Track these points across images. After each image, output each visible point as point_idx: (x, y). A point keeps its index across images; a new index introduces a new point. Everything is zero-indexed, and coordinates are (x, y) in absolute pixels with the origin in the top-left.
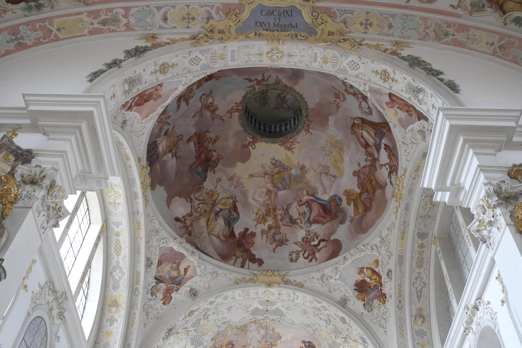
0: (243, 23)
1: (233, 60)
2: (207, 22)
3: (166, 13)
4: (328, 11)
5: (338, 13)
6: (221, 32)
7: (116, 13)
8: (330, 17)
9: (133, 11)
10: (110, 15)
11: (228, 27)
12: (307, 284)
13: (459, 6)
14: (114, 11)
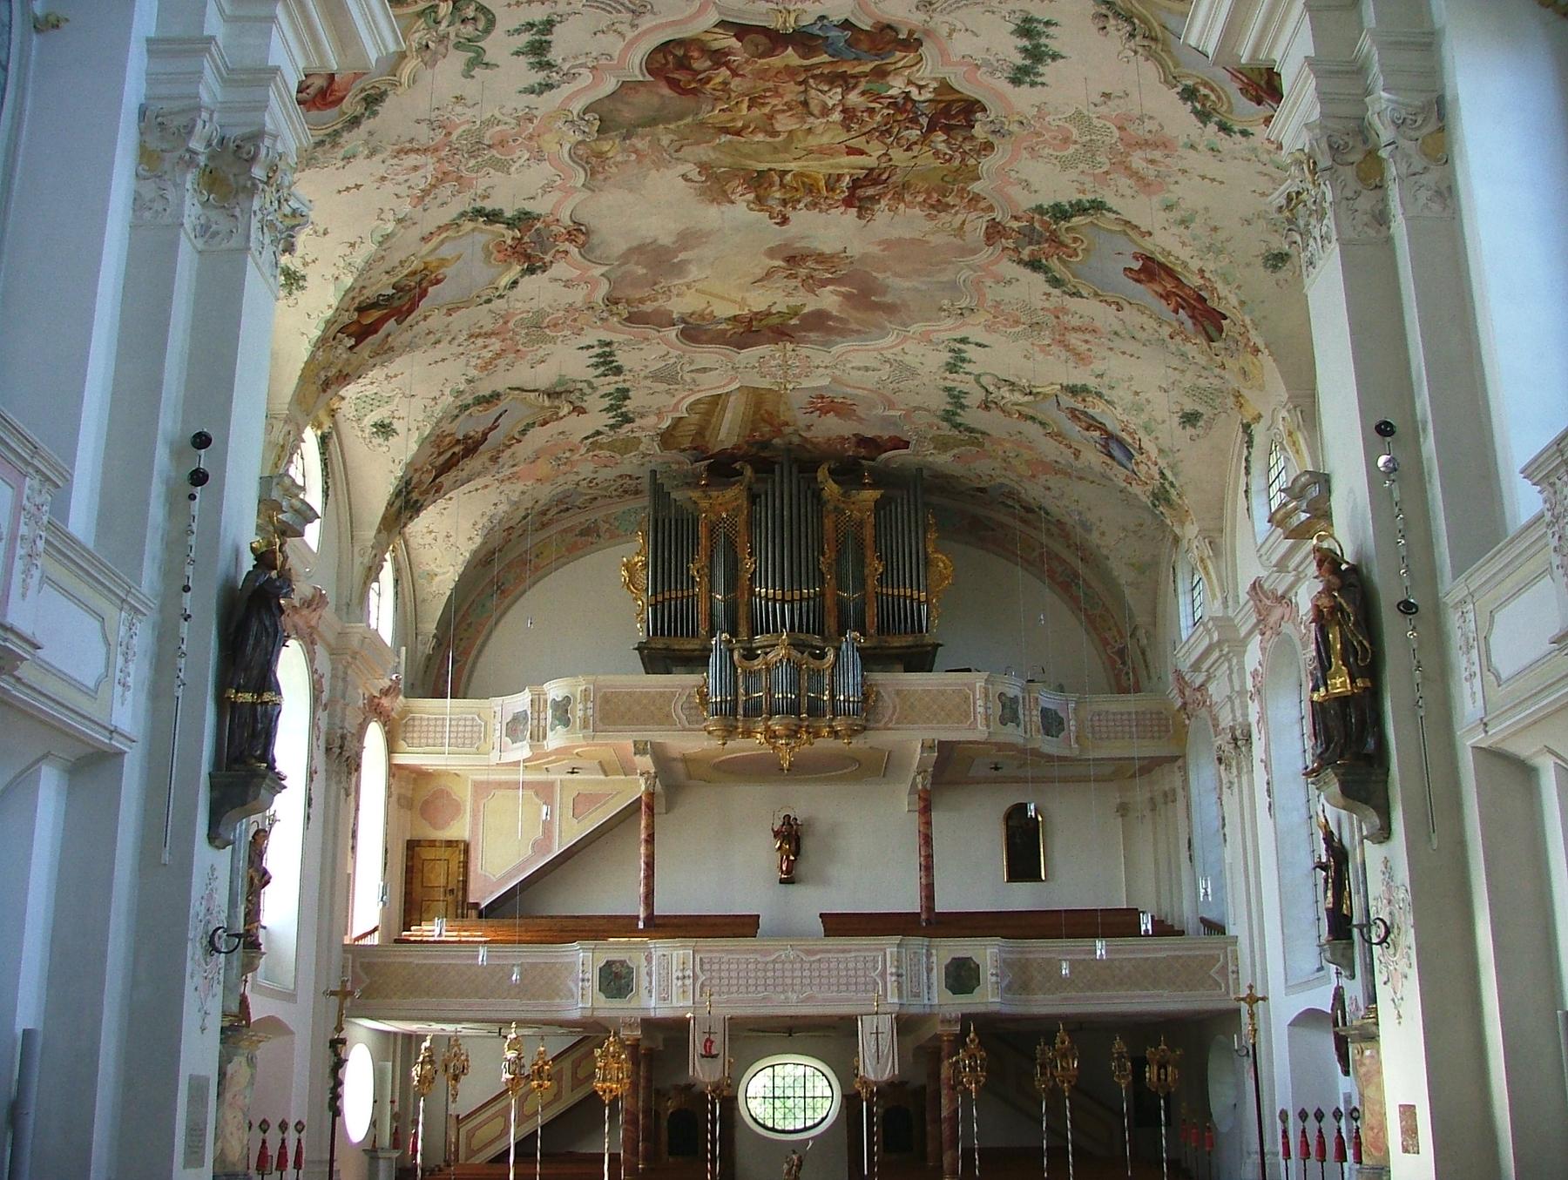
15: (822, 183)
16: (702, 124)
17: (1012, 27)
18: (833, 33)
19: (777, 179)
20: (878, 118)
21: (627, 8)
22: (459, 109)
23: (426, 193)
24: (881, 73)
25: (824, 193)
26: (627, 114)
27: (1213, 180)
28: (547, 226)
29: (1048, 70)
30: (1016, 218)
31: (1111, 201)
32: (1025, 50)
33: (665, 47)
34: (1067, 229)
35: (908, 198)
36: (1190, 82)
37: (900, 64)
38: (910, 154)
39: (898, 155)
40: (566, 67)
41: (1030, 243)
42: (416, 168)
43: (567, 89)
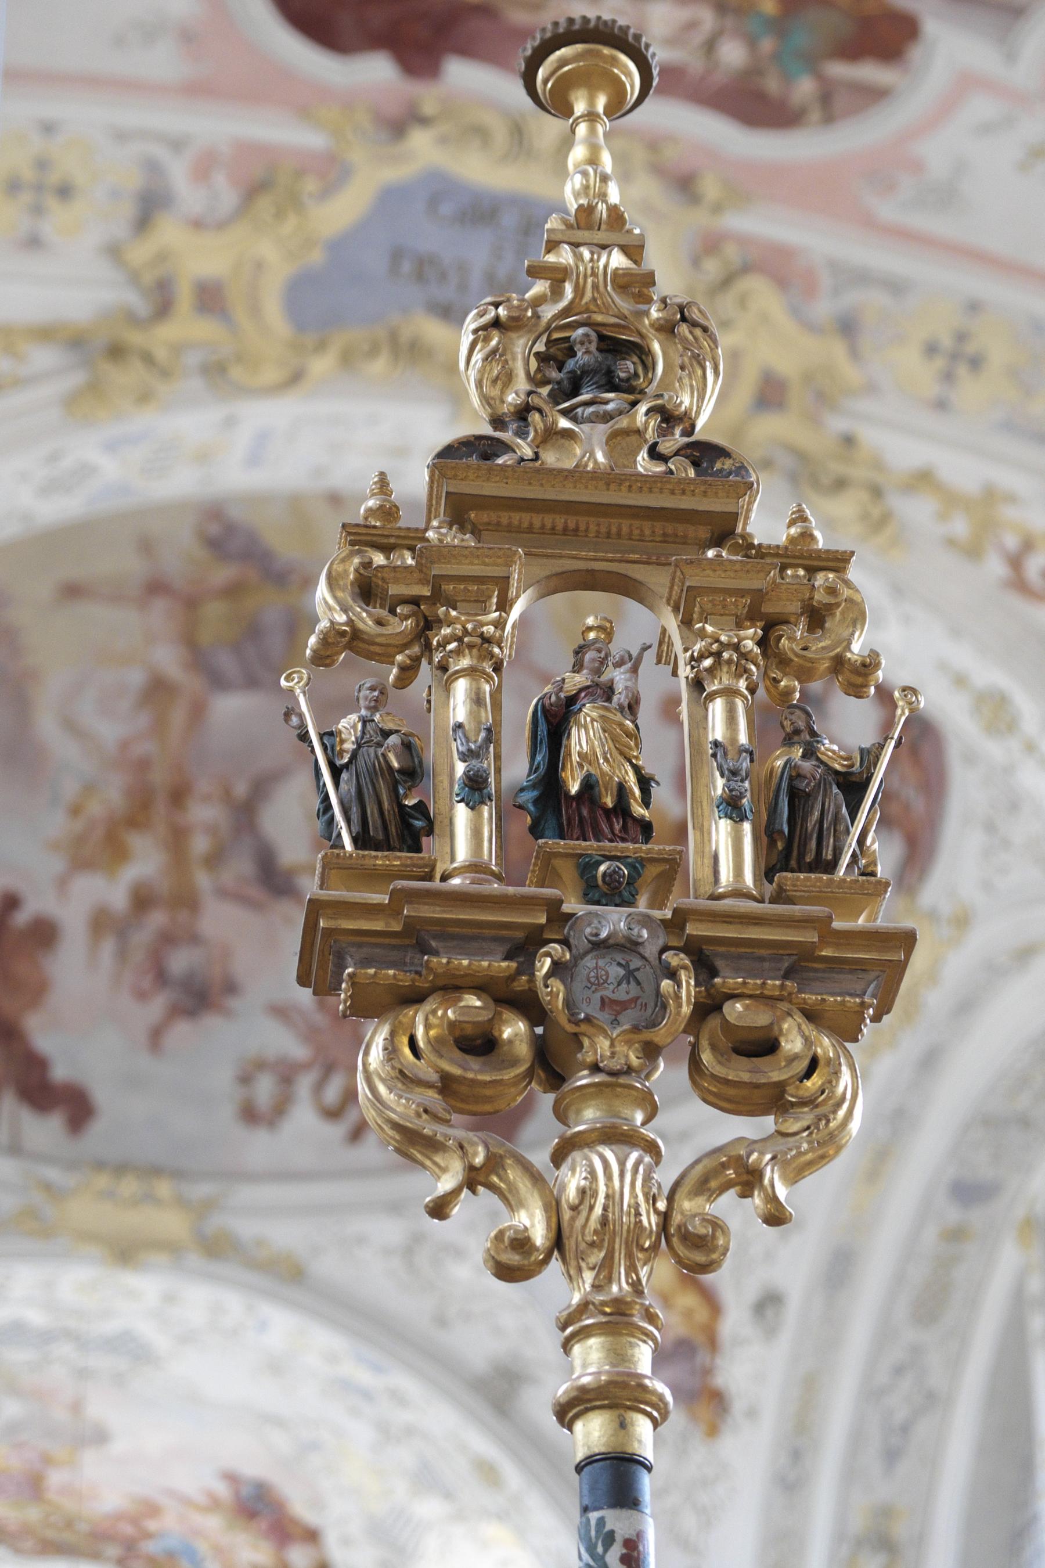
1: (254, 459)
4: (777, 266)
6: (210, 298)
8: (782, 282)
12: (328, 1266)
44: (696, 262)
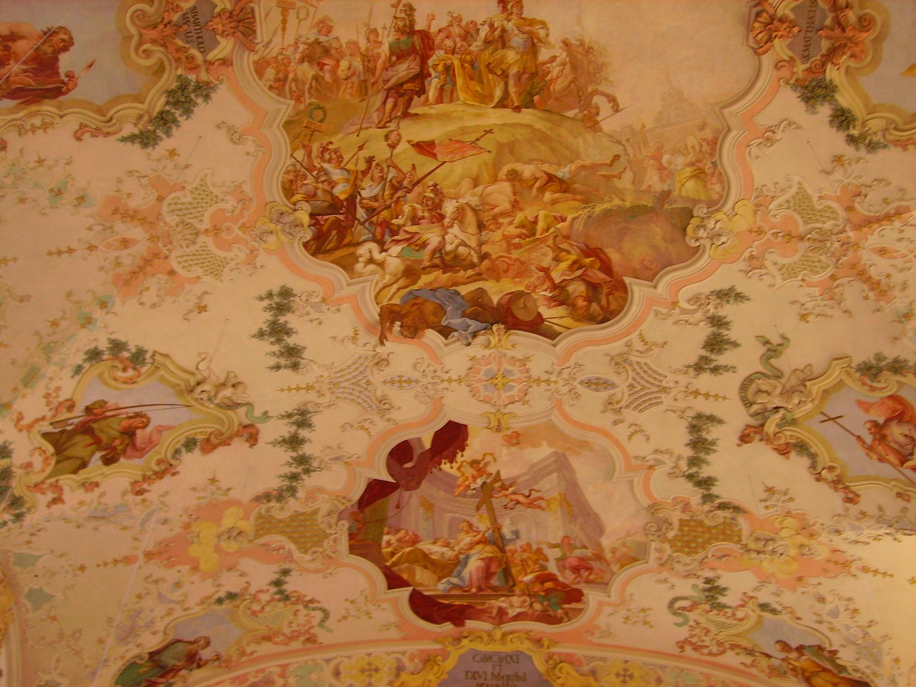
0: (449, 673)
2: (398, 675)
3: (339, 664)
4: (570, 660)
5: (584, 660)
7: (270, 673)
9: (291, 668)
10: (260, 676)
11: (427, 682)
13: (752, 666)
14: (267, 671)
15: (460, 81)
16: (586, 201)
17: (306, 355)
18: (456, 321)
19: (512, 90)
20: (407, 209)
21: (631, 365)
22: (809, 305)
23: (888, 217)
24: (411, 273)
25: (457, 63)
26: (657, 231)
27: (60, 253)
28: (792, 60)
29: (262, 318)
30: (225, 62)
31: (135, 155)
32: (289, 332)
33: (606, 316)
34: (160, 70)
35: (358, 64)
36: (144, 370)
37: (395, 287)
38: (365, 153)
39: (379, 149)
40: (699, 315)
41: (194, 9)
42: (882, 252)
43: (705, 287)
44: (547, 662)
